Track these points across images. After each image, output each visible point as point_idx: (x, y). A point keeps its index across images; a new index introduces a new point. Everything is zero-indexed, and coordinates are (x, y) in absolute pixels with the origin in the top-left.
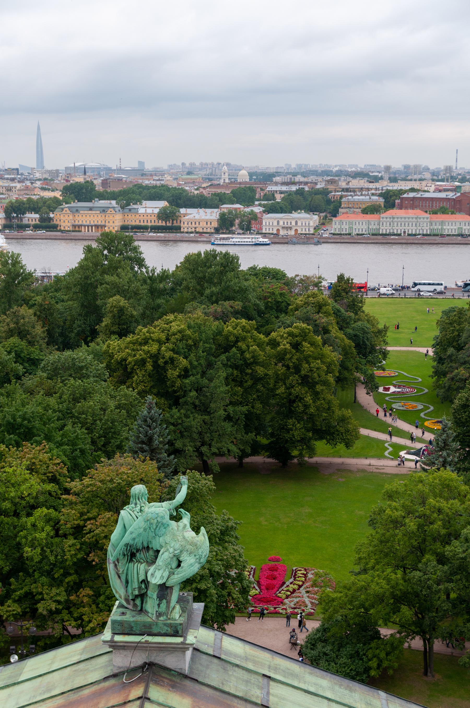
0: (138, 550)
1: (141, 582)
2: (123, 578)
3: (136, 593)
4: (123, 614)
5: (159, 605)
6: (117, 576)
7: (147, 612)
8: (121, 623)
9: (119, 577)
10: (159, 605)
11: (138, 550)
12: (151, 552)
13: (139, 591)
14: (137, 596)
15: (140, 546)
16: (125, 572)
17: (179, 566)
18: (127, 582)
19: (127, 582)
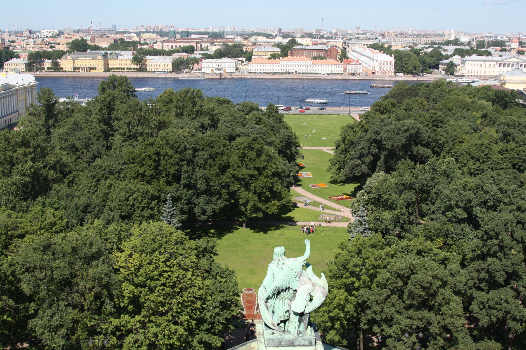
0: (282, 290)
1: (286, 312)
2: (271, 309)
3: (282, 319)
4: (273, 333)
5: (299, 326)
6: (266, 309)
7: (289, 332)
8: (273, 340)
9: (268, 309)
10: (299, 326)
11: (282, 290)
12: (291, 291)
13: (284, 318)
14: (281, 322)
15: (284, 288)
16: (273, 305)
17: (311, 300)
18: (273, 312)
19: (273, 312)
